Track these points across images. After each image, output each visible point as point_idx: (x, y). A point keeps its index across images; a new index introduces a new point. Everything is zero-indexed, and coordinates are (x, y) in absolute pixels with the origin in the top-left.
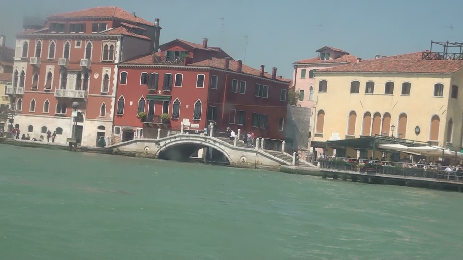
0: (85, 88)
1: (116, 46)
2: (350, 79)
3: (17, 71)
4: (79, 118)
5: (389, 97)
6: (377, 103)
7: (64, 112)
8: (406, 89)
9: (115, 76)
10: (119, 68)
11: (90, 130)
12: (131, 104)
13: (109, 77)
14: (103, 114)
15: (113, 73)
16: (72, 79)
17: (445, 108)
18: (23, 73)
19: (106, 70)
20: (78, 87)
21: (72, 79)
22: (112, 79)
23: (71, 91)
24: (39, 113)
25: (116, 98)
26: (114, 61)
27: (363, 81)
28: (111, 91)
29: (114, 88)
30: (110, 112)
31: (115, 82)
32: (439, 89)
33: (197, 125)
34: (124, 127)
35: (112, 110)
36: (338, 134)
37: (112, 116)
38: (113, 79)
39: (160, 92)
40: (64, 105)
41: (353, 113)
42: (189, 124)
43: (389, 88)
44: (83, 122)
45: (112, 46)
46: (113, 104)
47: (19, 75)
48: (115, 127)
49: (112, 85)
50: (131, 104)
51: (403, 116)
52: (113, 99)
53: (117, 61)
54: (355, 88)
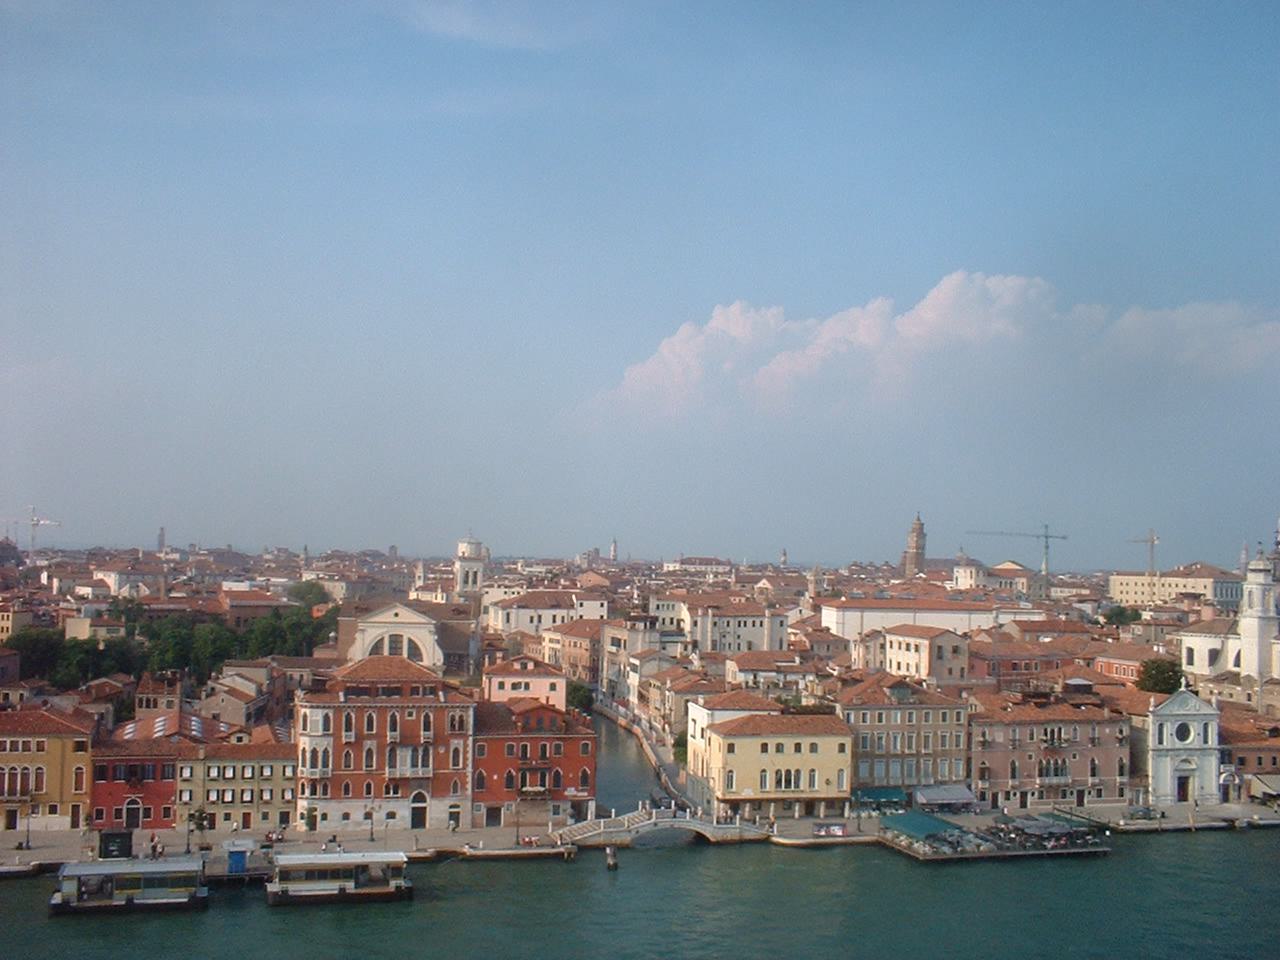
0: (425, 764)
1: (468, 716)
2: (758, 742)
3: (304, 749)
4: (420, 798)
5: (799, 755)
6: (788, 761)
7: (395, 792)
8: (814, 748)
9: (470, 749)
10: (475, 741)
11: (437, 810)
12: (495, 777)
13: (461, 750)
14: (455, 791)
15: (466, 746)
16: (404, 755)
17: (849, 762)
18: (326, 752)
19: (456, 743)
20: (414, 765)
21: (404, 755)
22: (465, 752)
23: (404, 768)
24: (358, 796)
25: (474, 773)
28: (465, 766)
29: (470, 762)
30: (467, 789)
31: (470, 755)
32: (842, 748)
33: (586, 794)
35: (469, 786)
37: (469, 792)
38: (467, 752)
39: (534, 763)
40: (397, 785)
42: (575, 793)
43: (798, 748)
44: (425, 801)
45: (461, 717)
46: (469, 779)
47: (320, 755)
49: (465, 759)
50: (495, 777)
52: (470, 775)
53: (471, 732)
54: (764, 748)
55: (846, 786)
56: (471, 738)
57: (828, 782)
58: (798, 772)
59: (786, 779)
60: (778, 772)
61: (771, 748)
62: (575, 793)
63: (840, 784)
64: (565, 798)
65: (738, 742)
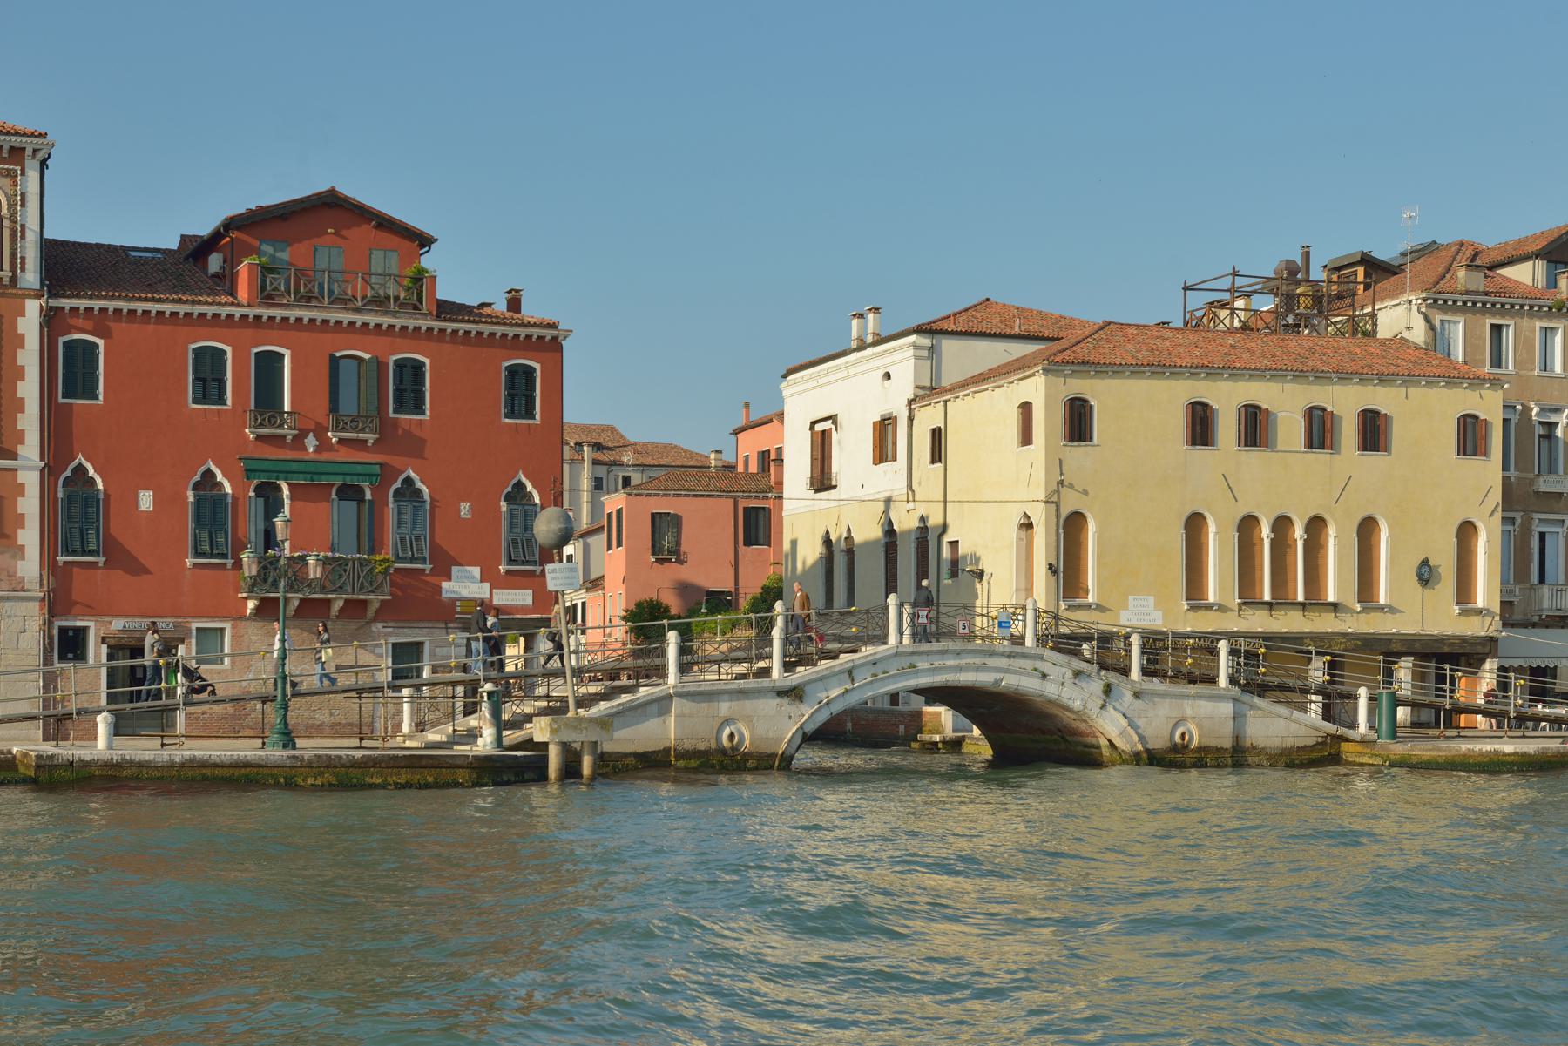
2: (1180, 392)
6: (1284, 481)
8: (1374, 431)
12: (146, 501)
26: (14, 280)
27: (1227, 398)
32: (1470, 436)
34: (117, 624)
35: (29, 537)
36: (1151, 599)
37: (30, 567)
41: (1195, 524)
43: (1320, 430)
46: (29, 505)
48: (58, 623)
50: (146, 501)
51: (1367, 528)
52: (30, 480)
54: (1200, 425)
55: (1486, 592)
56: (33, 307)
57: (1426, 575)
58: (1316, 525)
59: (1276, 551)
60: (1248, 524)
61: (1227, 427)
62: (480, 591)
63: (1464, 591)
64: (444, 613)
65: (1101, 393)
